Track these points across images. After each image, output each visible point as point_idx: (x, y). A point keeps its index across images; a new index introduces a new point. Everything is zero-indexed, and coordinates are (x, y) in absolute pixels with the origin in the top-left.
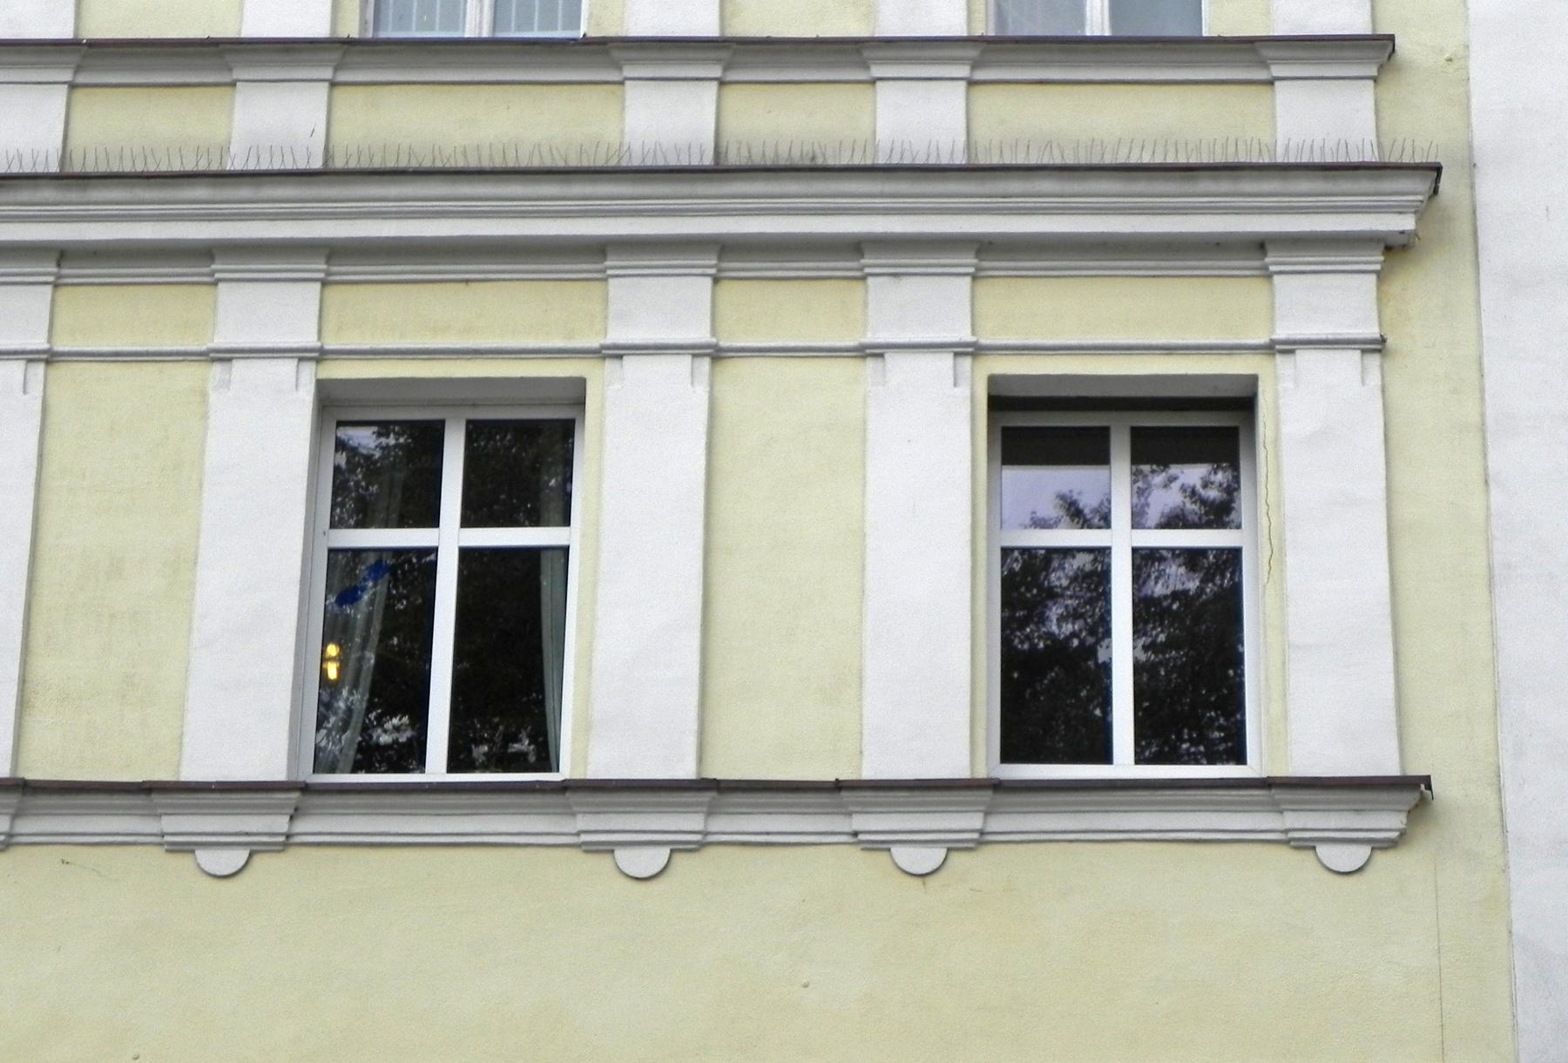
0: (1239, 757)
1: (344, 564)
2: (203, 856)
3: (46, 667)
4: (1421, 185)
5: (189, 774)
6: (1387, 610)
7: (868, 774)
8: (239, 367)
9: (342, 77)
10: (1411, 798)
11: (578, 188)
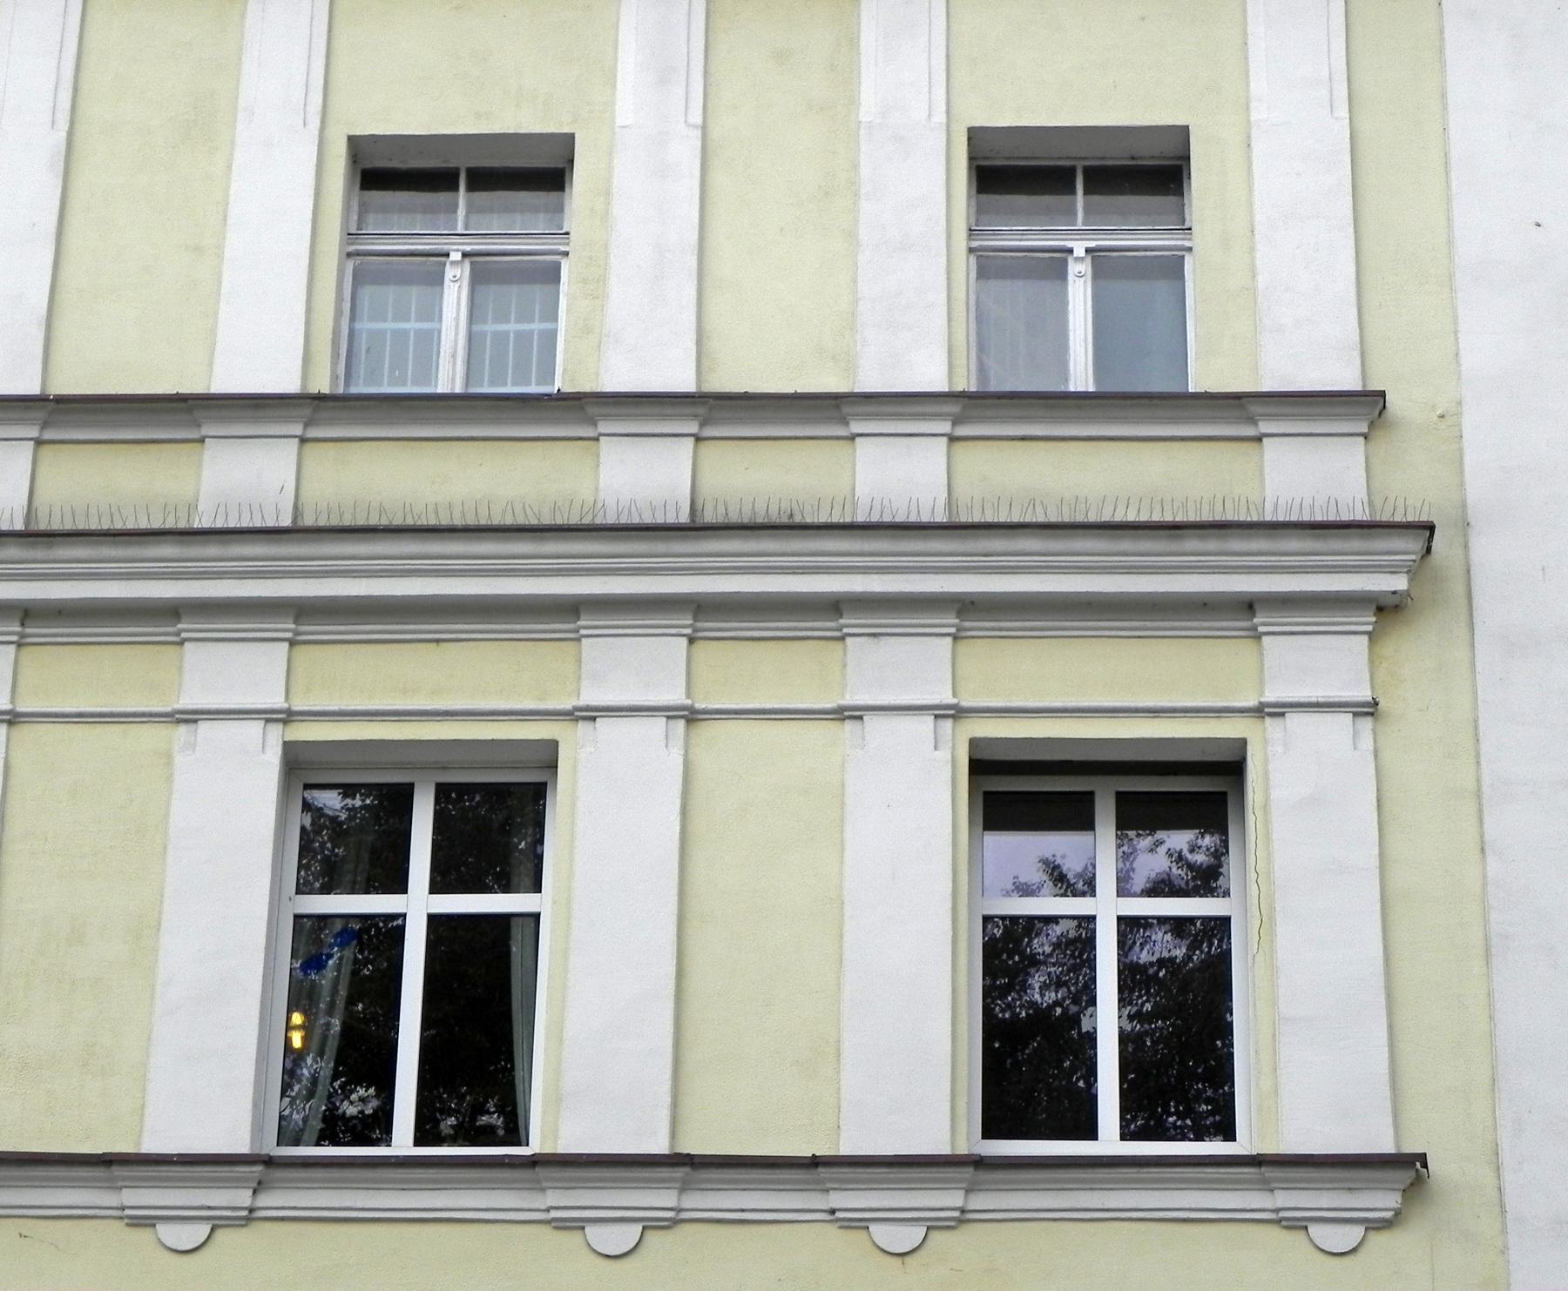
0: (1227, 1131)
2: (163, 1230)
4: (1414, 544)
5: (150, 1146)
6: (1380, 981)
7: (846, 1149)
8: (204, 727)
9: (313, 433)
10: (1406, 1176)
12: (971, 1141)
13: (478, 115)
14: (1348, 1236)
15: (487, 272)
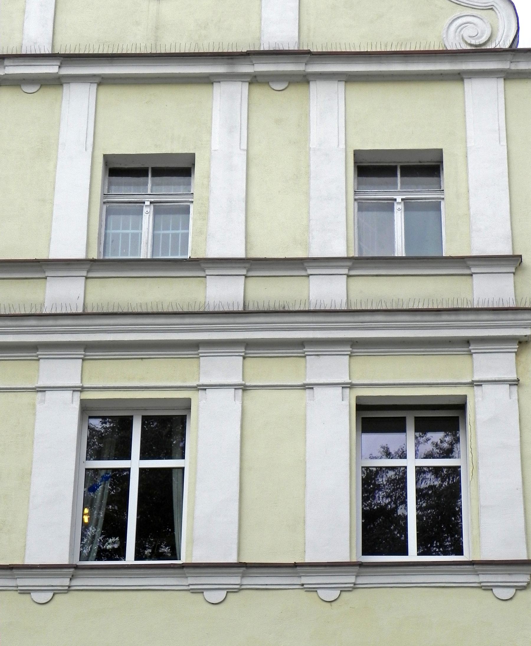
0: (460, 552)
2: (34, 595)
5: (28, 561)
7: (307, 560)
8: (48, 394)
9: (90, 275)
11: (187, 320)
12: (358, 557)
13: (156, 146)
14: (508, 593)
15: (159, 209)
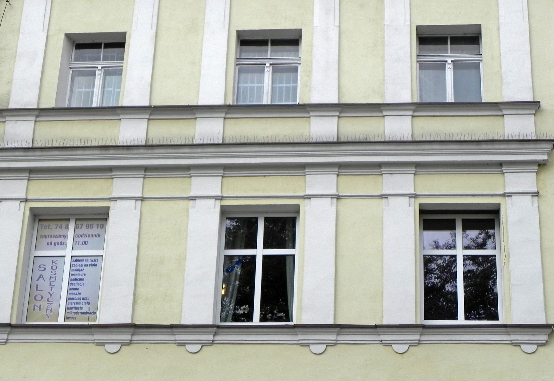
0: (496, 318)
1: (229, 259)
3: (141, 291)
7: (385, 323)
8: (198, 201)
9: (228, 116)
14: (533, 348)
15: (277, 69)
